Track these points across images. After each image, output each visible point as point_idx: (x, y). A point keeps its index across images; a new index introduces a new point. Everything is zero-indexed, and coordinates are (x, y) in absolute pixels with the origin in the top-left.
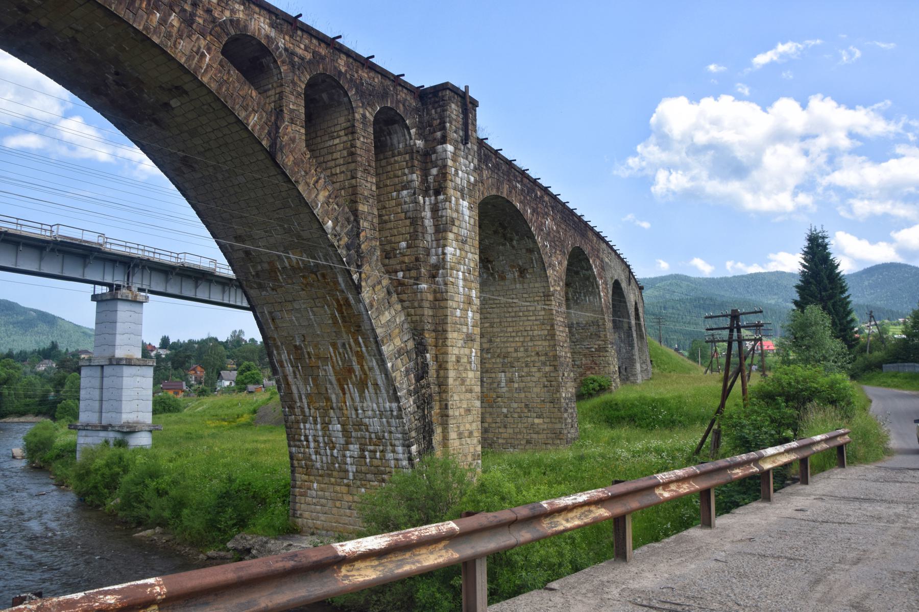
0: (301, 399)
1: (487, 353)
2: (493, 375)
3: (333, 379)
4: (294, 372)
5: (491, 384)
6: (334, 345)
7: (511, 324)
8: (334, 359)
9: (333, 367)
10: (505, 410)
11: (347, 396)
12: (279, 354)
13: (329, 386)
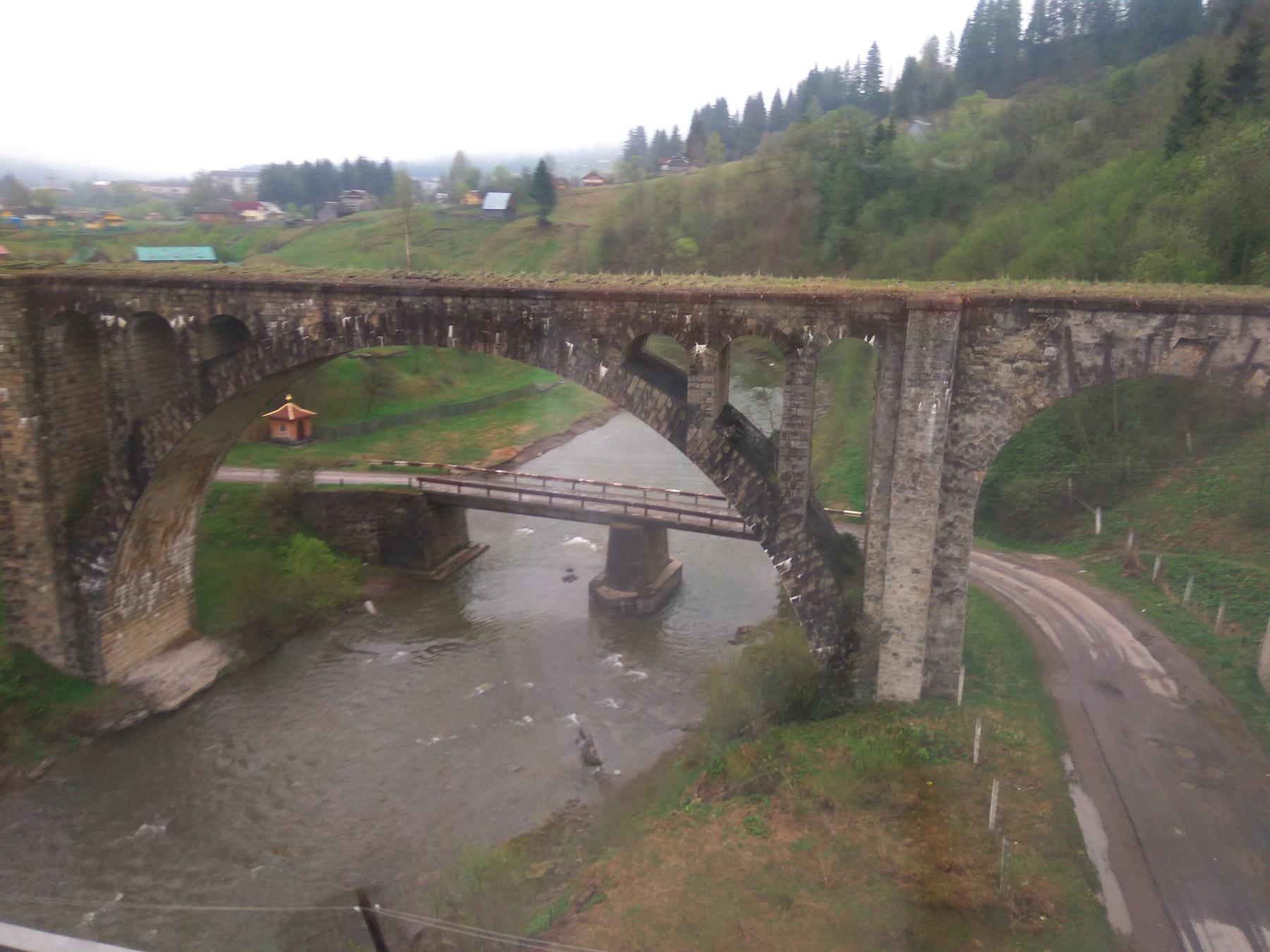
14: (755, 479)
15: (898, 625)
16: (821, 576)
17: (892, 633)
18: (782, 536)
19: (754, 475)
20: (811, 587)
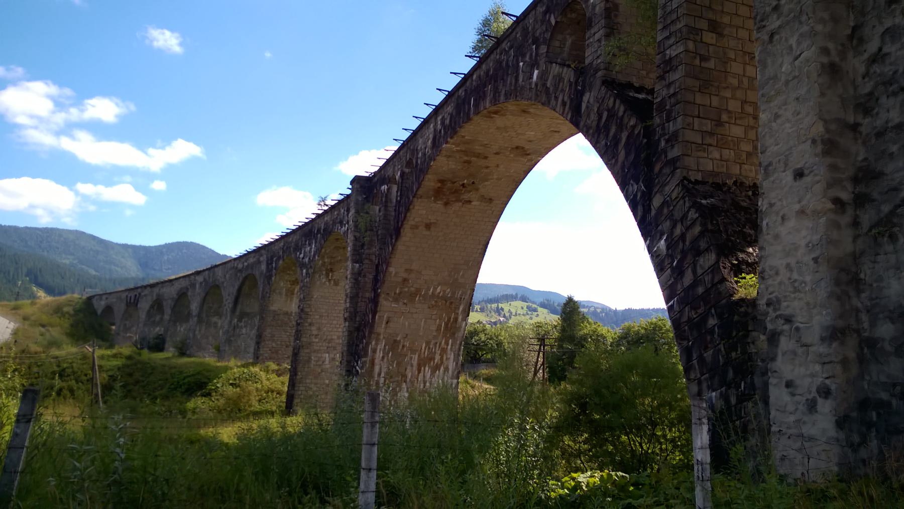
0: (379, 374)
1: (316, 338)
2: (319, 355)
3: (415, 363)
4: (383, 357)
5: (317, 361)
6: (428, 343)
7: (336, 319)
8: (423, 351)
9: (419, 356)
10: (327, 382)
11: (420, 374)
12: (377, 344)
13: (409, 368)
14: (634, 127)
15: (788, 312)
16: (698, 253)
17: (780, 333)
18: (657, 202)
19: (632, 122)
20: (688, 279)
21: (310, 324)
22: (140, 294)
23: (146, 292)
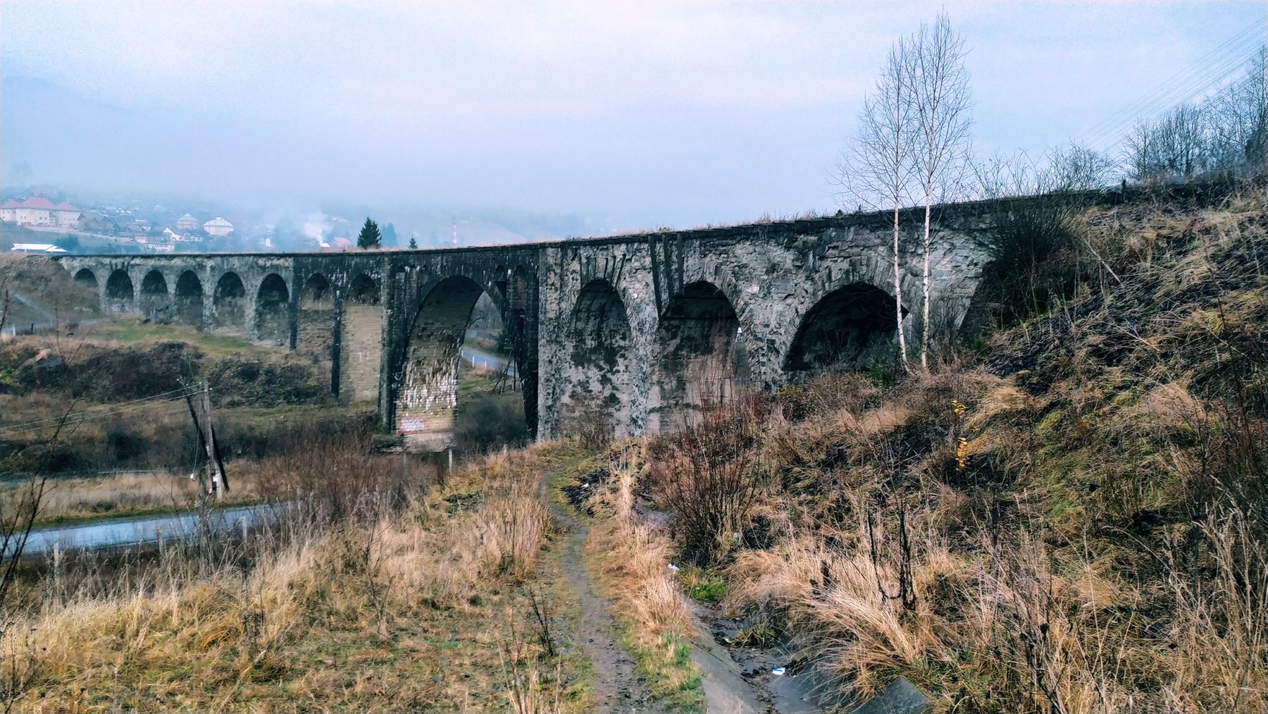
10: (362, 372)
21: (347, 333)
22: (129, 263)
23: (137, 261)
